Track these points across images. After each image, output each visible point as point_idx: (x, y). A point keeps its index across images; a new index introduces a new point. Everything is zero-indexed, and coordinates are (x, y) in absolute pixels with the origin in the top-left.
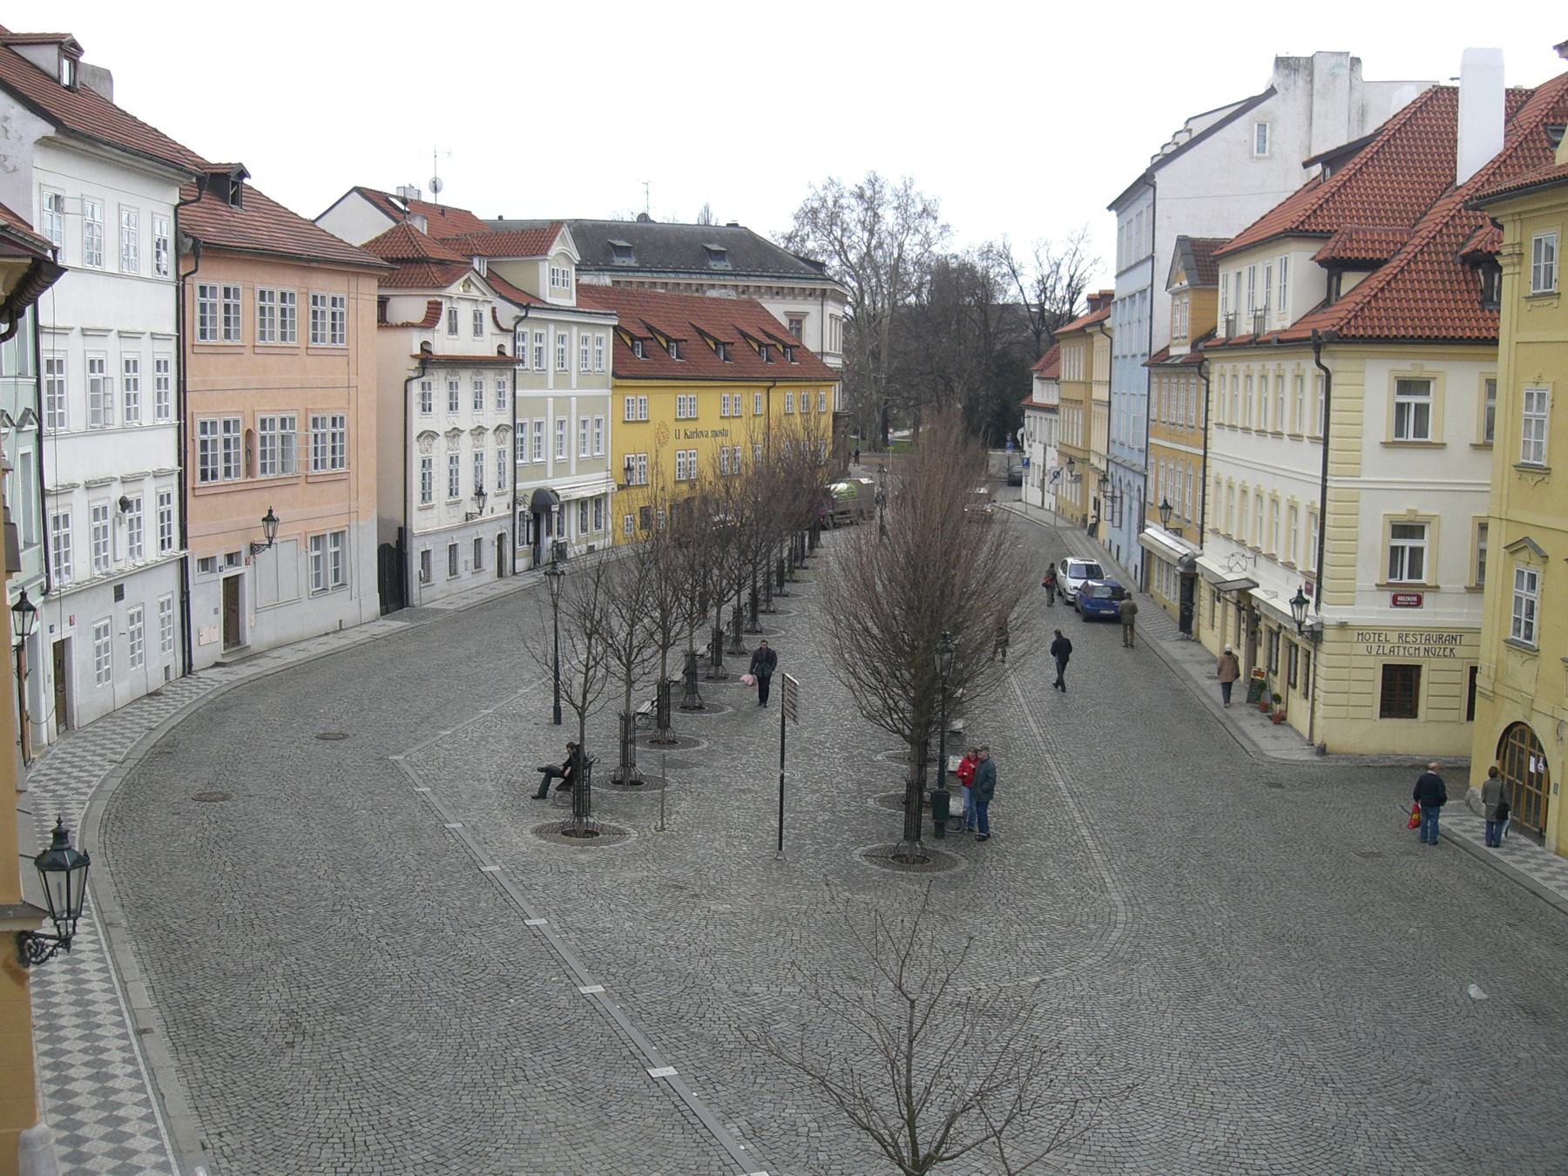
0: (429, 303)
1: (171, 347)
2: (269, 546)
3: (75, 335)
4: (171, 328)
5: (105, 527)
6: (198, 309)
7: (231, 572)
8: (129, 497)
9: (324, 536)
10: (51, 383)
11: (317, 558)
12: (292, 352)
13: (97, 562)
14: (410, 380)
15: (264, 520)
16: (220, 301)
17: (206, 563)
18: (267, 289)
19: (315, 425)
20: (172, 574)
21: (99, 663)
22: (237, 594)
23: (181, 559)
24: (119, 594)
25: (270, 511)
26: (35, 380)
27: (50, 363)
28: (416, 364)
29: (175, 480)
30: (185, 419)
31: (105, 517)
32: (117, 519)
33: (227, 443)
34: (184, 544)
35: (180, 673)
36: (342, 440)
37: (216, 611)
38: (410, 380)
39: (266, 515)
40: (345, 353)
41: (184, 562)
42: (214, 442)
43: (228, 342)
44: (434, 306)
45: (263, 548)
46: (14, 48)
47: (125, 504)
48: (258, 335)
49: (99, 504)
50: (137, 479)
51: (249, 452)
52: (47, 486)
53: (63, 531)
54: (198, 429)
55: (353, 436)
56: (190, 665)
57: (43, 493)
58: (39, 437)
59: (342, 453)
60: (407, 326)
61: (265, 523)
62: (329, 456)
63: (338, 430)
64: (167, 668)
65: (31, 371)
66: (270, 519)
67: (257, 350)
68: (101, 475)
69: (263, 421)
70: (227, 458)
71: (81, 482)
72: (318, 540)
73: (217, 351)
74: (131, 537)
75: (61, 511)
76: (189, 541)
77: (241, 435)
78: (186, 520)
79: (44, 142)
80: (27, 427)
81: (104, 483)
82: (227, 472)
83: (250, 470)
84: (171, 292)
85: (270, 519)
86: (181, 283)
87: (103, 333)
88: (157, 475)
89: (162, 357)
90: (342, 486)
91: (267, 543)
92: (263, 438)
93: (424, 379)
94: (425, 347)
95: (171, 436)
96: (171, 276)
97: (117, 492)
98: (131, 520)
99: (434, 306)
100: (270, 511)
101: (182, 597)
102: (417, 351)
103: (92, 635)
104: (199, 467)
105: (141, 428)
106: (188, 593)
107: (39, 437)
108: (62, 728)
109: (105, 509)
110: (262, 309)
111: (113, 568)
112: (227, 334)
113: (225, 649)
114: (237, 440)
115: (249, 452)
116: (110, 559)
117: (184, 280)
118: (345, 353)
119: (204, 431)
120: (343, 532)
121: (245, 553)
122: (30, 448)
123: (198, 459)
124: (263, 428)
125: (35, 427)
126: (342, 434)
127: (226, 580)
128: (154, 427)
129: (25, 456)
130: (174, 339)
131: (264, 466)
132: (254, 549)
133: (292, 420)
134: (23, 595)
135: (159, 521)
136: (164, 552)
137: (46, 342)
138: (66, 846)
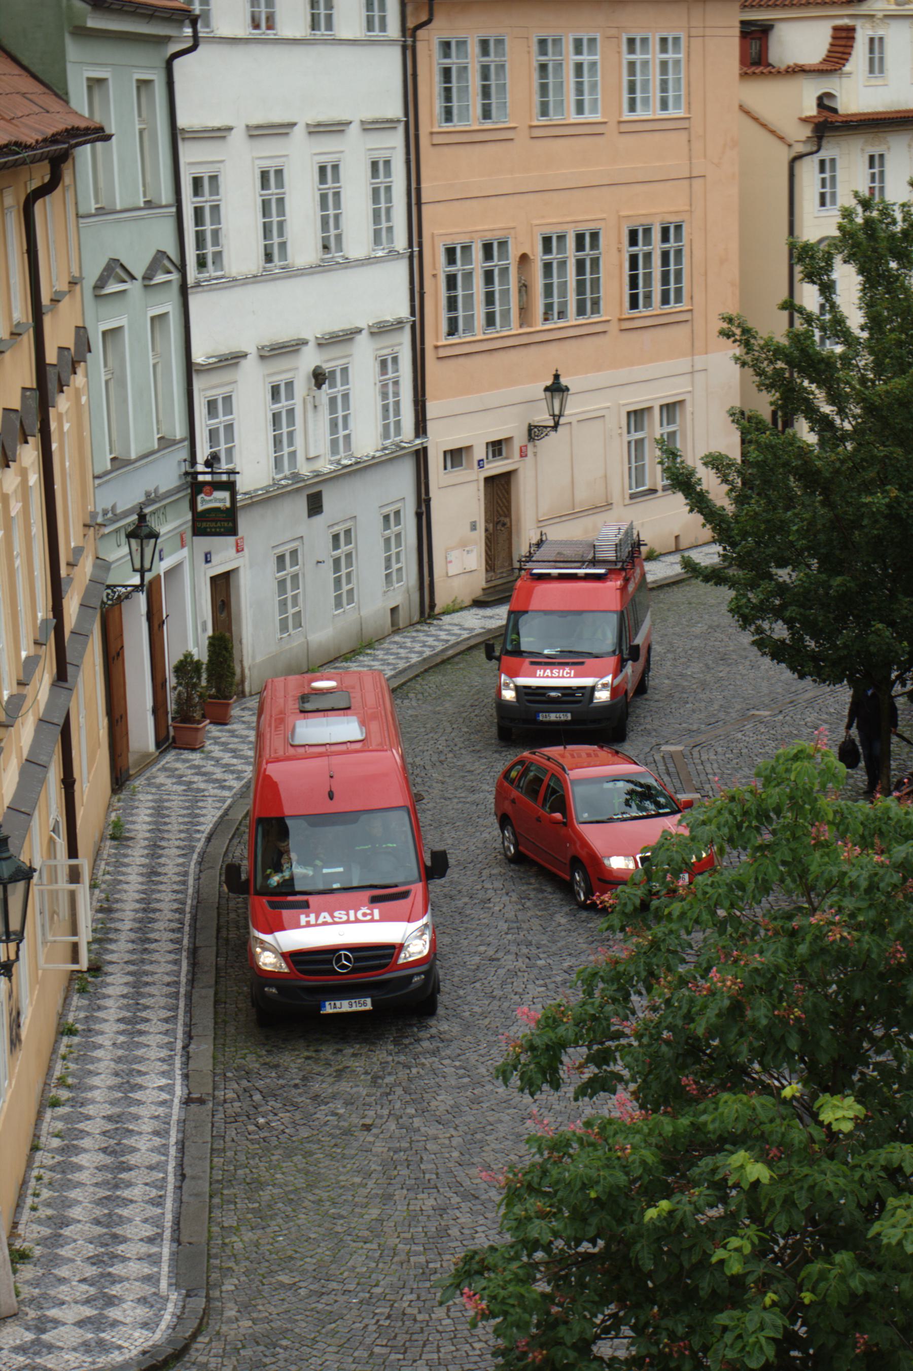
0: (836, 29)
1: (395, 141)
2: (555, 427)
3: (238, 137)
4: (395, 110)
5: (291, 412)
6: (437, 77)
7: (497, 467)
8: (327, 367)
9: (650, 409)
10: (198, 213)
11: (639, 443)
12: (594, 131)
13: (278, 462)
14: (799, 157)
15: (547, 389)
16: (473, 59)
17: (455, 456)
18: (548, 33)
19: (633, 241)
20: (405, 473)
21: (283, 604)
22: (509, 501)
23: (417, 451)
24: (315, 505)
25: (557, 377)
26: (174, 209)
27: (197, 183)
28: (806, 131)
29: (406, 337)
30: (420, 245)
31: (290, 395)
32: (309, 399)
33: (489, 276)
34: (421, 427)
35: (416, 618)
36: (678, 260)
37: (474, 527)
38: (799, 157)
39: (549, 383)
40: (685, 124)
41: (421, 457)
42: (468, 276)
43: (488, 125)
44: (844, 34)
45: (546, 431)
47: (319, 378)
48: (536, 109)
49: (281, 379)
50: (346, 337)
51: (524, 288)
52: (198, 357)
53: (222, 419)
54: (442, 258)
55: (698, 254)
56: (432, 606)
57: (189, 368)
58: (184, 291)
59: (678, 279)
60: (798, 71)
61: (548, 394)
62: (657, 288)
63: (672, 245)
65: (166, 196)
66: (556, 389)
67: (537, 133)
68: (284, 335)
69: (547, 241)
70: (490, 298)
71: (252, 350)
72: (637, 417)
73: (471, 140)
74: (334, 424)
75: (218, 393)
76: (430, 425)
77: (512, 262)
78: (424, 395)
80: (160, 278)
82: (490, 320)
83: (525, 311)
84: (395, 54)
85: (556, 389)
86: (409, 40)
87: (282, 130)
88: (380, 330)
89: (381, 156)
90: (681, 332)
91: (552, 423)
92: (548, 267)
93: (822, 154)
94: (826, 102)
95: (399, 271)
96: (393, 30)
97: (310, 359)
98: (333, 401)
99: (844, 34)
100: (557, 377)
101: (419, 505)
102: (811, 109)
103: (273, 564)
104: (444, 315)
105: (348, 264)
106: (428, 501)
107: (184, 291)
109: (290, 385)
110: (543, 67)
111: (304, 469)
112: (487, 114)
113: (487, 582)
114: (504, 271)
115: (524, 288)
116: (300, 457)
117: (414, 36)
118: (685, 124)
119: (451, 260)
120: (681, 402)
121: (520, 438)
122: (169, 305)
123: (443, 302)
124: (547, 248)
125: (175, 276)
126: (679, 252)
127: (489, 480)
128: (369, 261)
129: (158, 320)
130: (401, 128)
131: (549, 307)
132: (534, 433)
133: (595, 236)
134: (142, 517)
135: (379, 398)
136: (388, 442)
137: (189, 153)
138: (5, 855)
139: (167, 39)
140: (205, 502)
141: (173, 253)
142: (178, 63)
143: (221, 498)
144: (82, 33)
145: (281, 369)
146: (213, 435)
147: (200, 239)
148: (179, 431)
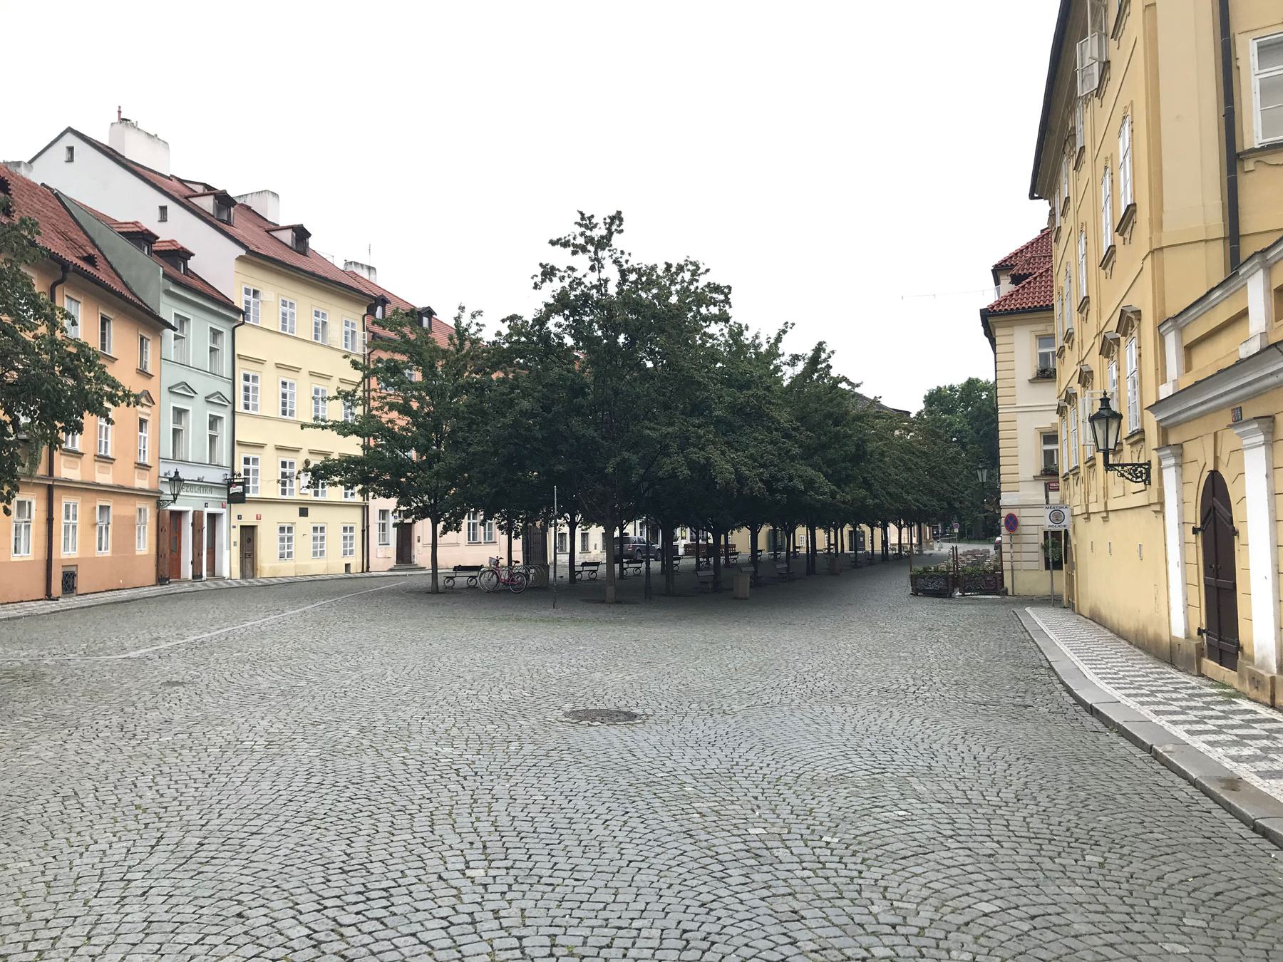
10: (247, 389)
24: (303, 513)
46: (273, 233)
56: (368, 567)
58: (233, 412)
64: (347, 566)
79: (240, 259)
81: (296, 450)
106: (368, 527)
108: (248, 572)
122: (225, 414)
125: (230, 407)
139: (234, 320)
140: (233, 490)
141: (227, 394)
142: (237, 329)
143: (239, 489)
144: (169, 293)
145: (288, 457)
146: (247, 472)
147: (247, 398)
148: (225, 461)
